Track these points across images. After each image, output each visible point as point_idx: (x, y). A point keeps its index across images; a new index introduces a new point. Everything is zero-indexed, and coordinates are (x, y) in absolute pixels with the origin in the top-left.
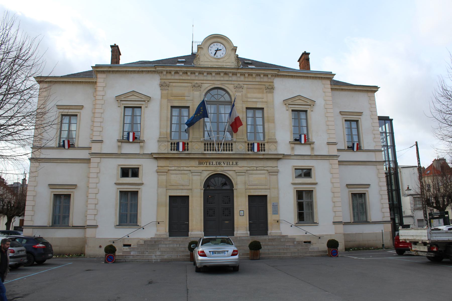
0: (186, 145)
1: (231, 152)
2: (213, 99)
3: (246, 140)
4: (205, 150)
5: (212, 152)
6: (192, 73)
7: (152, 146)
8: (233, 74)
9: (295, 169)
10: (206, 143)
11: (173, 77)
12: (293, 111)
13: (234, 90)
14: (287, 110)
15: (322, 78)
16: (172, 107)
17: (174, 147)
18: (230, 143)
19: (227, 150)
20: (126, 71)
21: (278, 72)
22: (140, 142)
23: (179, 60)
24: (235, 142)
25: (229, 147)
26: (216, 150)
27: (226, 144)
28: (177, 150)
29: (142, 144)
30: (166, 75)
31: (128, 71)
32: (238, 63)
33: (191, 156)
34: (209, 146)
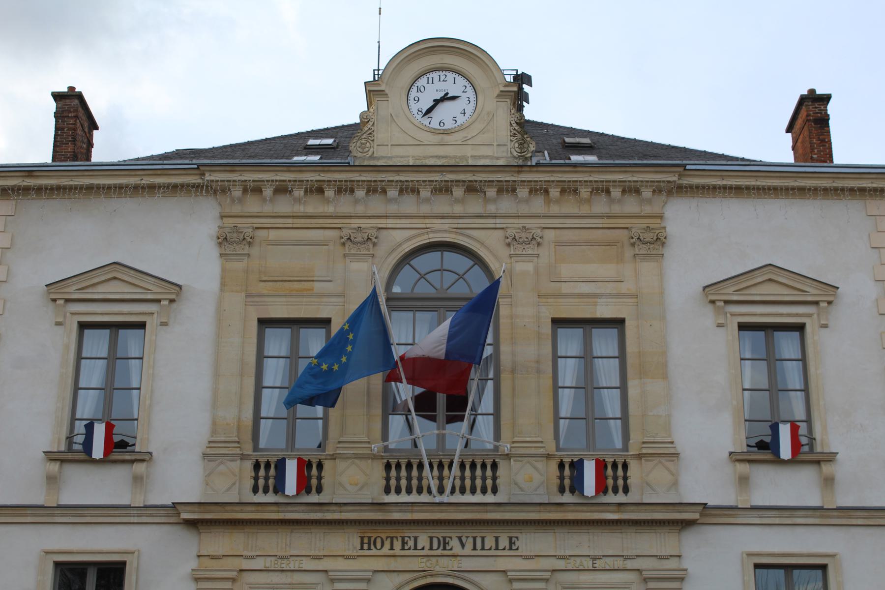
0: (314, 471)
1: (489, 498)
2: (423, 289)
3: (551, 448)
4: (387, 490)
5: (414, 498)
6: (339, 191)
7: (180, 477)
8: (500, 191)
9: (757, 566)
10: (393, 462)
11: (268, 209)
12: (742, 327)
13: (504, 252)
14: (720, 325)
15: (862, 190)
16: (264, 323)
17: (267, 478)
18: (489, 462)
19: (473, 491)
20: (90, 188)
21: (681, 176)
22: (132, 462)
23: (311, 142)
24: (508, 457)
25: (484, 479)
26: (429, 492)
27: (473, 466)
28: (276, 492)
29: (139, 468)
30: (240, 200)
31: (99, 187)
32: (522, 144)
33: (329, 516)
34: (404, 473)
